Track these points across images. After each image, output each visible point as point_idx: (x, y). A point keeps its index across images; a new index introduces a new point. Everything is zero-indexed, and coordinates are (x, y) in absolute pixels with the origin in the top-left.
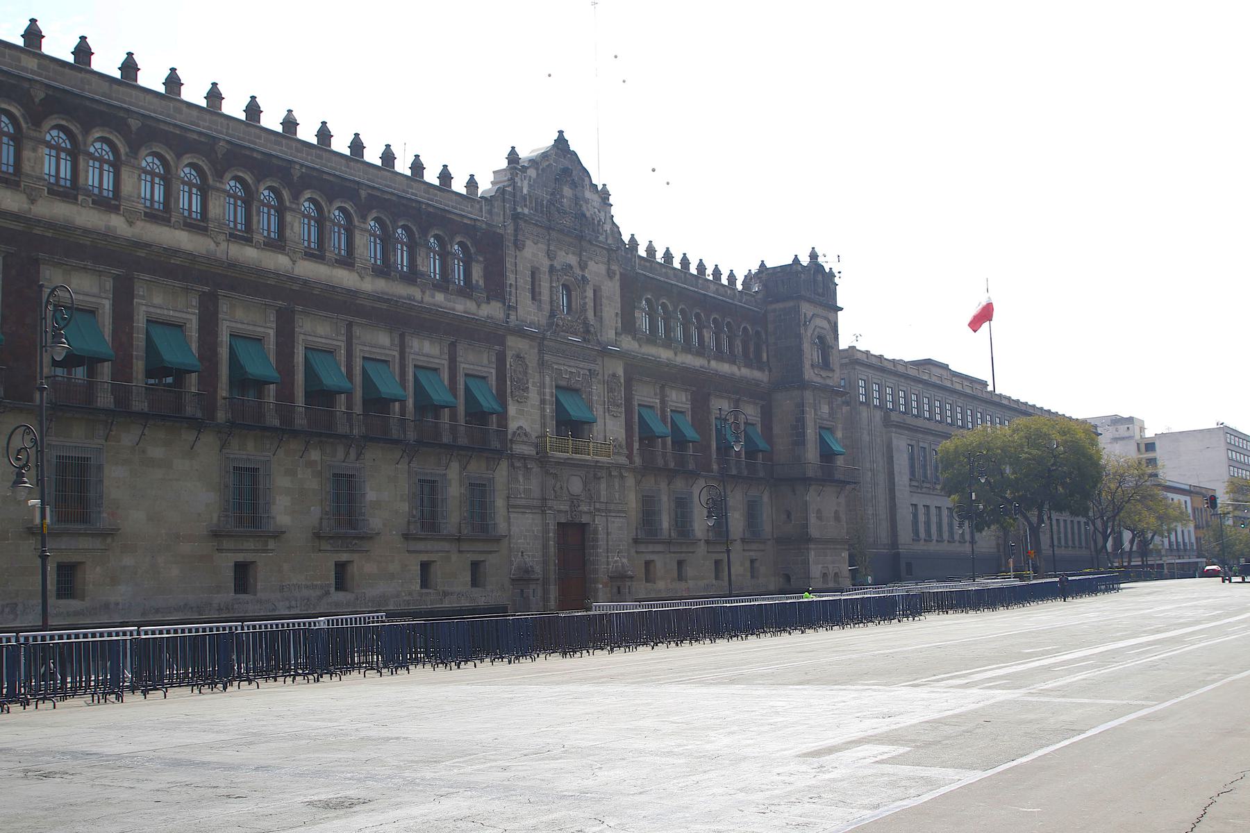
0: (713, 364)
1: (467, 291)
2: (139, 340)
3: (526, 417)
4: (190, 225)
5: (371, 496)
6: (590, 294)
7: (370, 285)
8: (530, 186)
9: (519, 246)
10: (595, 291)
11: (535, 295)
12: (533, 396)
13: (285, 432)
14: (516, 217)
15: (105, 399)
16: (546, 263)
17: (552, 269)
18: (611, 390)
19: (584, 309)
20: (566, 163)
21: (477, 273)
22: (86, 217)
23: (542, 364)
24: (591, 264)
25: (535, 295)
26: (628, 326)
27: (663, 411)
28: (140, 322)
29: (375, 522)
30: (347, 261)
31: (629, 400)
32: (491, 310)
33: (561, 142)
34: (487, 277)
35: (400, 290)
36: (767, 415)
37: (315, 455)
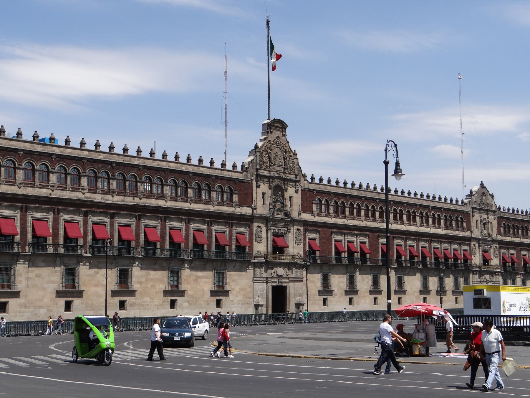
1: (463, 229)
3: (476, 260)
8: (476, 199)
9: (473, 216)
11: (477, 227)
14: (473, 208)
17: (481, 221)
18: (495, 251)
20: (483, 190)
23: (479, 247)
25: (477, 227)
26: (499, 233)
27: (508, 255)
29: (447, 289)
31: (500, 253)
32: (467, 234)
33: (482, 184)
34: (467, 225)
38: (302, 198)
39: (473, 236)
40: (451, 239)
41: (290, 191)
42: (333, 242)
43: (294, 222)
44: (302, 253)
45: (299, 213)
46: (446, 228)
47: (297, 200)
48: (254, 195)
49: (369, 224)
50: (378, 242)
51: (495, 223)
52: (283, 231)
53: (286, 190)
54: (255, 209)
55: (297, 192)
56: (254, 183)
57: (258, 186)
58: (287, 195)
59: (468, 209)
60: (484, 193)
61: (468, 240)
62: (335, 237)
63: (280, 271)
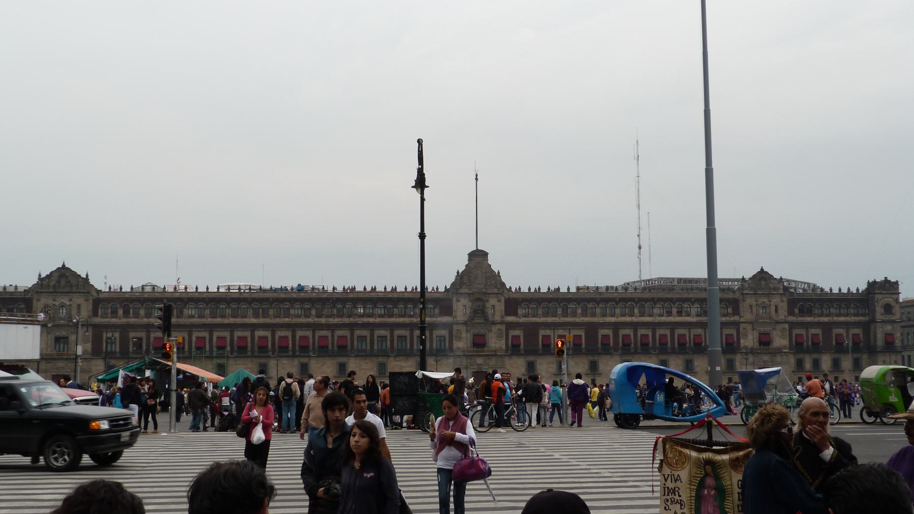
0: (835, 318)
2: (639, 339)
5: (696, 364)
6: (773, 308)
9: (744, 301)
10: (776, 307)
12: (750, 337)
13: (673, 352)
15: (632, 351)
16: (755, 303)
19: (770, 313)
20: (763, 275)
21: (730, 310)
22: (628, 319)
24: (774, 300)
26: (791, 313)
27: (807, 335)
28: (639, 335)
29: (697, 369)
32: (736, 318)
33: (762, 269)
36: (867, 332)
37: (681, 356)
39: (742, 320)
41: (493, 301)
42: (540, 337)
43: (494, 323)
44: (504, 347)
45: (502, 317)
46: (698, 315)
47: (500, 307)
48: (455, 307)
49: (586, 319)
50: (597, 333)
51: (783, 306)
52: (482, 332)
53: (488, 301)
54: (455, 317)
56: (454, 299)
57: (458, 301)
58: (489, 305)
59: (737, 295)
60: (762, 278)
61: (736, 325)
62: (542, 332)
63: (480, 361)
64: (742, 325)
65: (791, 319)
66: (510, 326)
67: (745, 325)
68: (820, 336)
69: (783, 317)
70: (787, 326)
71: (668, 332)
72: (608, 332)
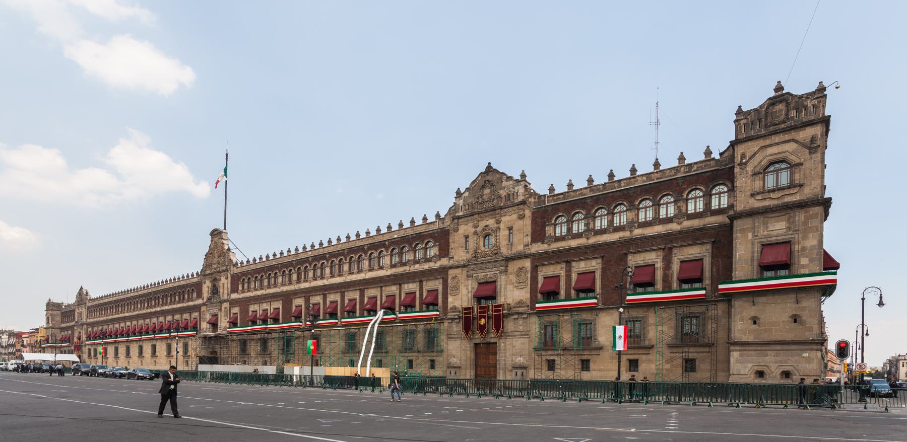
4: (339, 276)
7: (390, 272)
30: (381, 268)
32: (444, 262)
35: (399, 270)
38: (232, 283)
40: (397, 280)
41: (223, 279)
45: (228, 295)
46: (393, 266)
55: (227, 278)
58: (221, 284)
61: (444, 271)
62: (253, 308)
64: (451, 272)
65: (539, 248)
66: (233, 303)
67: (458, 271)
68: (598, 275)
69: (520, 248)
70: (527, 264)
71: (356, 295)
72: (299, 302)
